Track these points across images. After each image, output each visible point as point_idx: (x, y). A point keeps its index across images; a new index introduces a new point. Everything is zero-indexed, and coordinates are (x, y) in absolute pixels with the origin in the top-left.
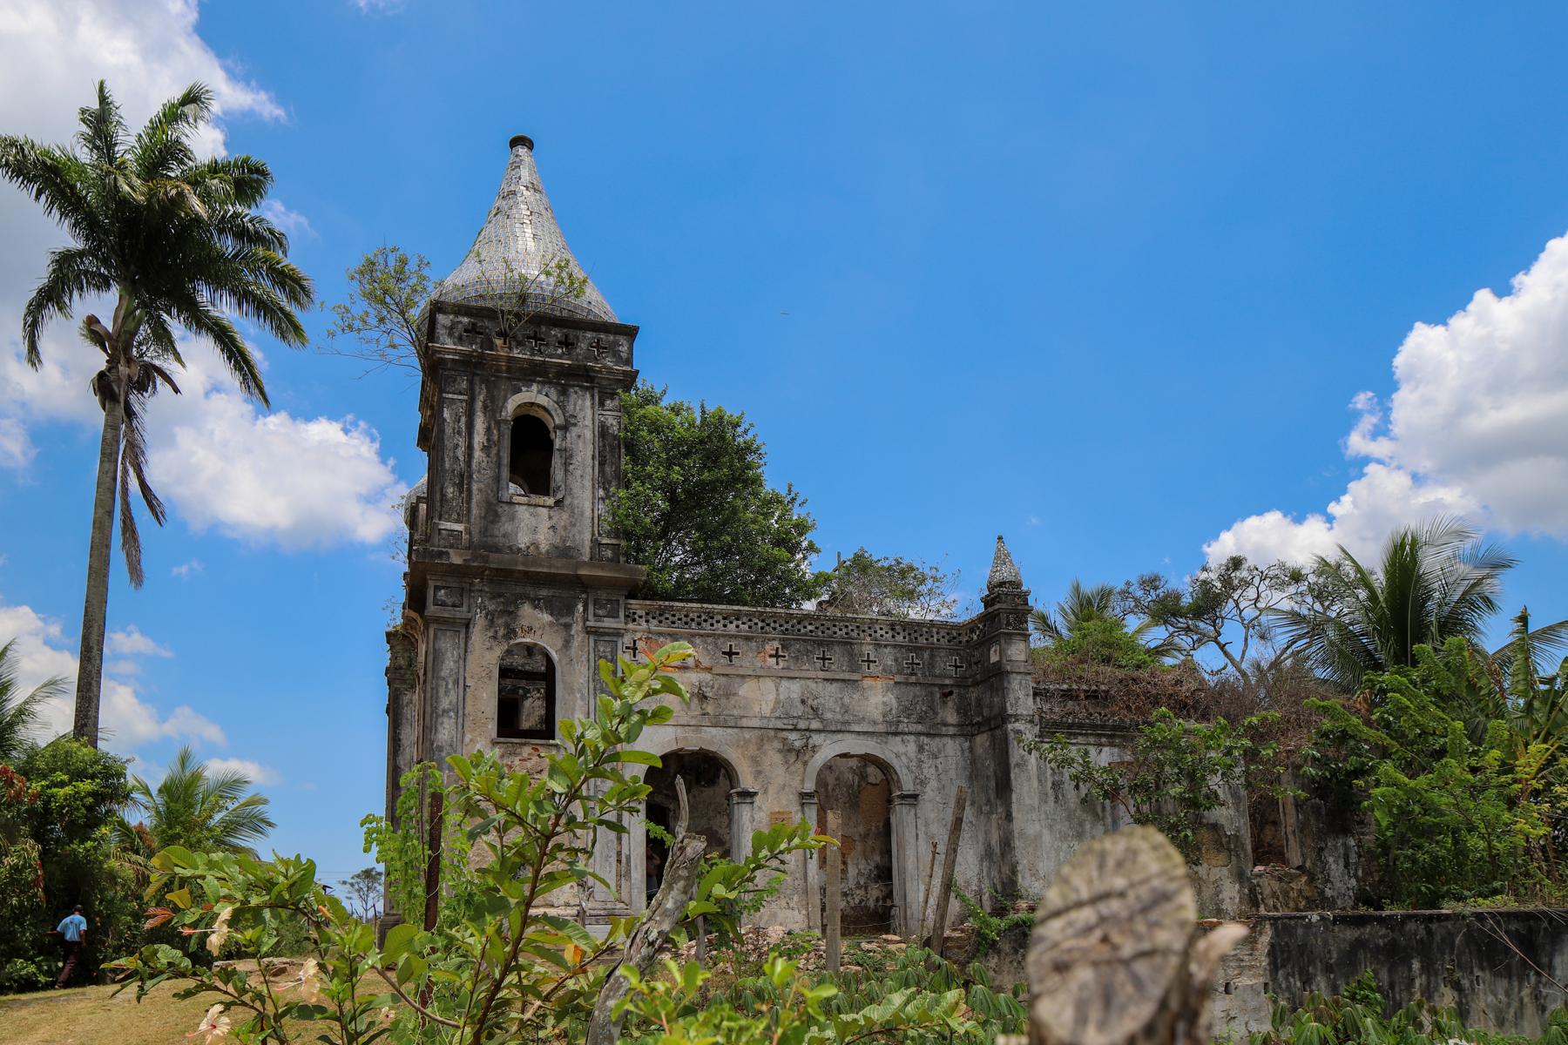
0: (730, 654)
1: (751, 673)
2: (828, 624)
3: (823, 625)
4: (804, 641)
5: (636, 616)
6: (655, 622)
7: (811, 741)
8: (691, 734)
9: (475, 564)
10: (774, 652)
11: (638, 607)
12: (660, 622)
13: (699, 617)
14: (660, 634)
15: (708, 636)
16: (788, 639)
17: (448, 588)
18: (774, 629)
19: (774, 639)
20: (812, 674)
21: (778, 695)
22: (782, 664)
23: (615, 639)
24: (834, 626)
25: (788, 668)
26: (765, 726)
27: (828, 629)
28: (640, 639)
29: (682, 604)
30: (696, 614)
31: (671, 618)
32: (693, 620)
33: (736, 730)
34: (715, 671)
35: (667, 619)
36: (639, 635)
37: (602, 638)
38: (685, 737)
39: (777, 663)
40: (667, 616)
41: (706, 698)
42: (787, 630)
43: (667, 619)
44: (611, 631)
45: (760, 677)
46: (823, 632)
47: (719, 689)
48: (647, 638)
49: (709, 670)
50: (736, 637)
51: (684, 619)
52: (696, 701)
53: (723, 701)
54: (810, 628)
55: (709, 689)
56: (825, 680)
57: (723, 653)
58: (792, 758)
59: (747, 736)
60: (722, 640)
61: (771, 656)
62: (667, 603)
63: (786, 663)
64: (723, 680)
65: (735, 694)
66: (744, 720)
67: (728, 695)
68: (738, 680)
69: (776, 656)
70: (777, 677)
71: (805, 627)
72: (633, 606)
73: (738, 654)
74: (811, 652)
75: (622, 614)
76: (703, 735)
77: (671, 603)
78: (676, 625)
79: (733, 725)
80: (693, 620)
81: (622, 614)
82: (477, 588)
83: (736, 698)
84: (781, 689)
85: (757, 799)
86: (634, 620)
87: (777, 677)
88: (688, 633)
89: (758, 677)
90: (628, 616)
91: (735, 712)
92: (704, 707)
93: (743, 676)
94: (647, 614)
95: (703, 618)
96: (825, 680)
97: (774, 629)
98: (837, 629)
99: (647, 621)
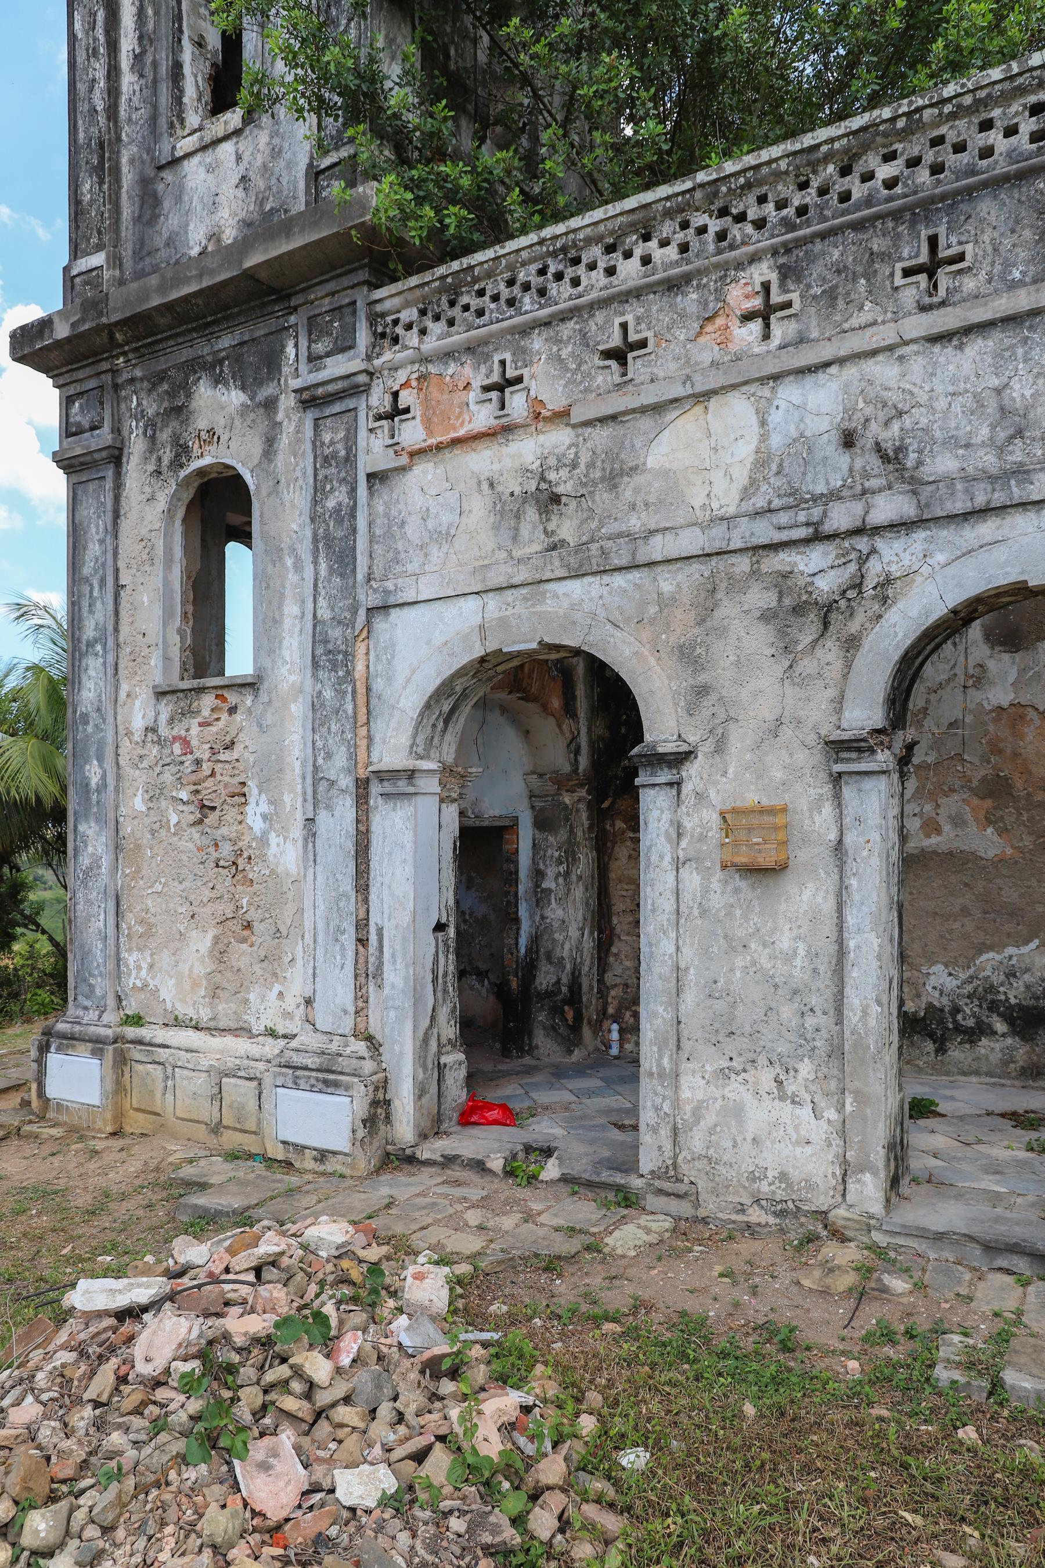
0: (618, 355)
1: (678, 391)
2: (963, 128)
3: (937, 142)
4: (858, 226)
5: (399, 330)
6: (436, 328)
7: (874, 569)
8: (520, 609)
9: (86, 327)
10: (757, 303)
11: (397, 301)
12: (451, 323)
13: (542, 272)
14: (448, 355)
15: (563, 317)
16: (799, 243)
17: (81, 394)
18: (760, 224)
19: (754, 259)
20: (886, 335)
21: (764, 438)
22: (779, 331)
23: (351, 403)
24: (986, 125)
25: (801, 340)
26: (718, 545)
27: (960, 148)
28: (406, 385)
29: (490, 253)
30: (533, 268)
31: (475, 303)
32: (526, 287)
33: (635, 575)
34: (578, 414)
35: (466, 308)
36: (402, 376)
37: (328, 412)
38: (501, 619)
39: (766, 336)
40: (465, 299)
41: (556, 499)
42: (802, 211)
43: (466, 308)
44: (340, 385)
45: (714, 392)
46: (937, 169)
47: (591, 465)
48: (422, 378)
49: (562, 416)
50: (637, 293)
51: (505, 293)
52: (531, 513)
53: (603, 497)
54: (885, 172)
55: (564, 473)
56: (935, 339)
57: (607, 354)
58: (807, 633)
59: (667, 587)
60: (600, 316)
61: (748, 317)
62: (455, 265)
63: (792, 328)
64: (601, 436)
65: (634, 469)
66: (657, 540)
67: (612, 480)
68: (645, 423)
69: (765, 314)
70: (763, 380)
71: (868, 177)
72: (388, 305)
73: (643, 344)
74: (885, 257)
75: (363, 337)
76: (549, 606)
77: (465, 261)
78: (486, 318)
79: (624, 561)
80: (526, 287)
81: (363, 337)
82: (125, 376)
83: (638, 479)
84: (775, 418)
85: (693, 772)
86: (396, 340)
87: (763, 380)
88: (512, 330)
89: (703, 397)
90: (383, 335)
91: (635, 523)
92: (551, 526)
93: (657, 409)
94: (423, 312)
95: (552, 270)
96: (935, 339)
97: (760, 224)
98: (995, 137)
99: (423, 332)
